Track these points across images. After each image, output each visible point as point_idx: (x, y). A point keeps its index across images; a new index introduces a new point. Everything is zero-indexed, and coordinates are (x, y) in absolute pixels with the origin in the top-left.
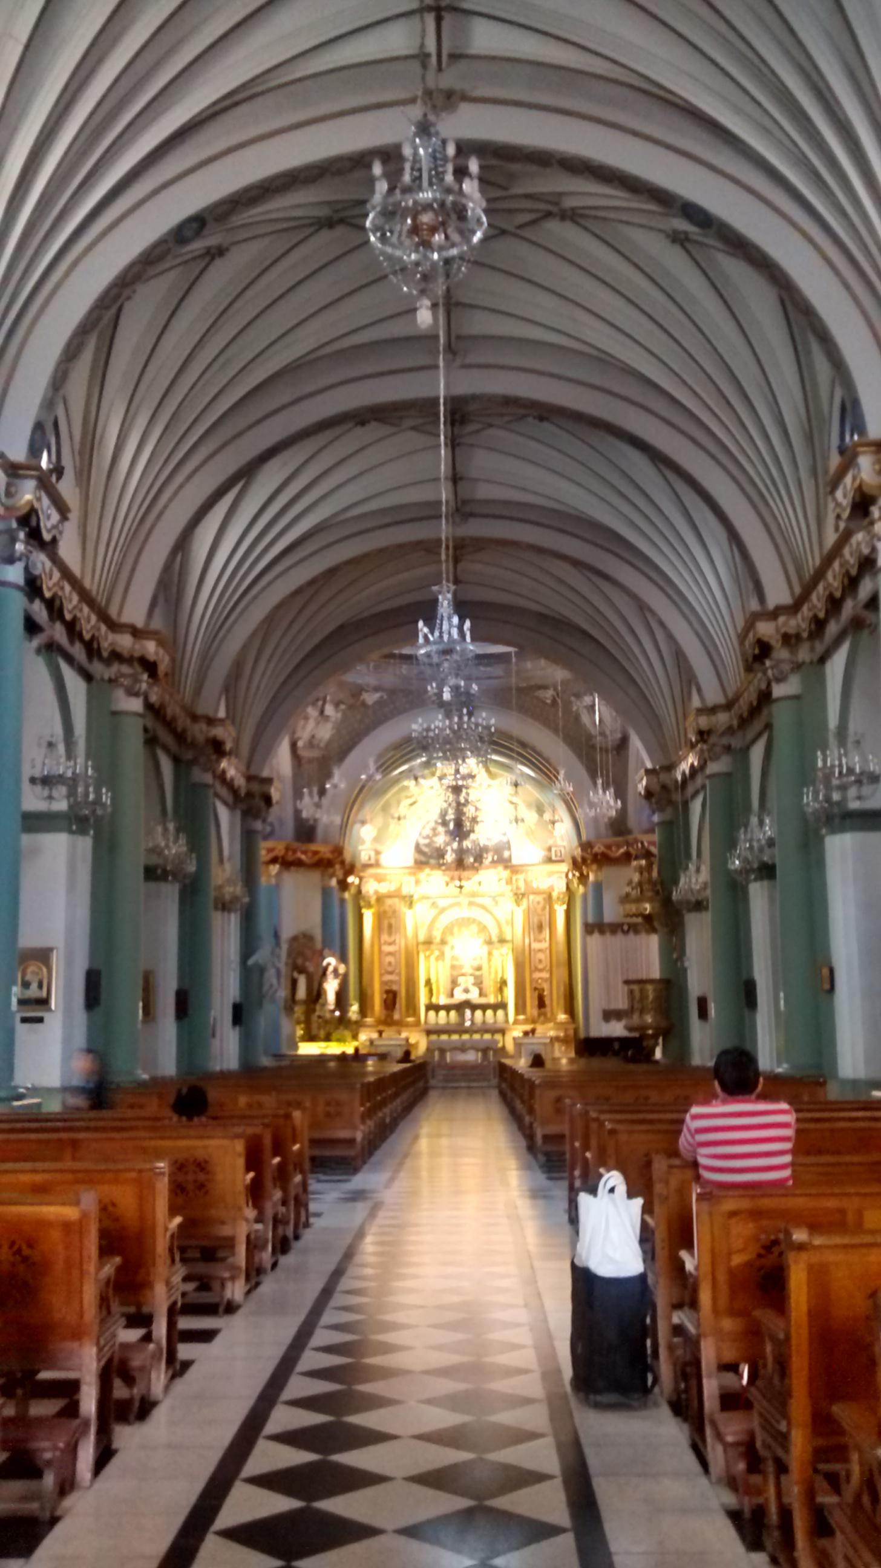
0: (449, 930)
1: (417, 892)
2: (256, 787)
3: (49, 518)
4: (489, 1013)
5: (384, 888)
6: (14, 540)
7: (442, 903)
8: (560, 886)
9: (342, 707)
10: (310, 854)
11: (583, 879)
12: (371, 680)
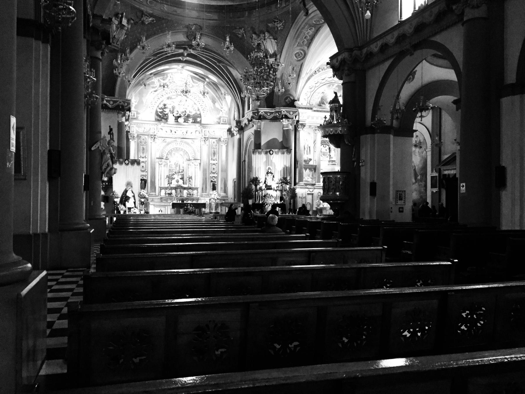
0: (170, 152)
1: (160, 134)
5: (141, 131)
7: (168, 140)
9: (132, 22)
10: (112, 103)
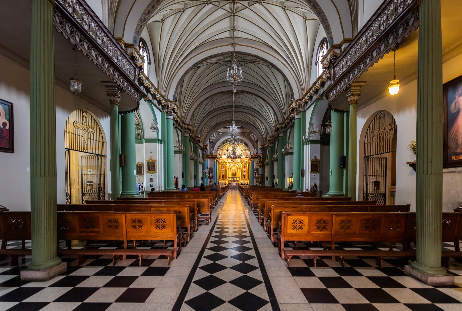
2: (204, 147)
3: (176, 109)
4: (237, 179)
5: (222, 161)
6: (171, 112)
7: (231, 163)
8: (248, 161)
11: (251, 160)
12: (221, 131)
